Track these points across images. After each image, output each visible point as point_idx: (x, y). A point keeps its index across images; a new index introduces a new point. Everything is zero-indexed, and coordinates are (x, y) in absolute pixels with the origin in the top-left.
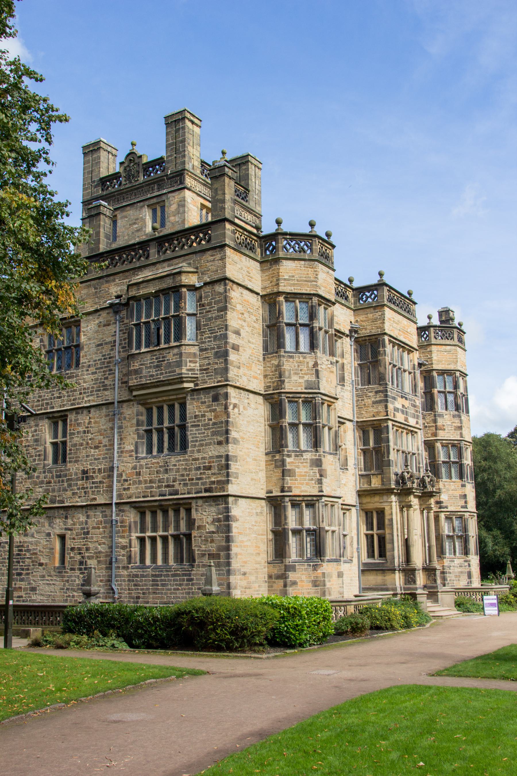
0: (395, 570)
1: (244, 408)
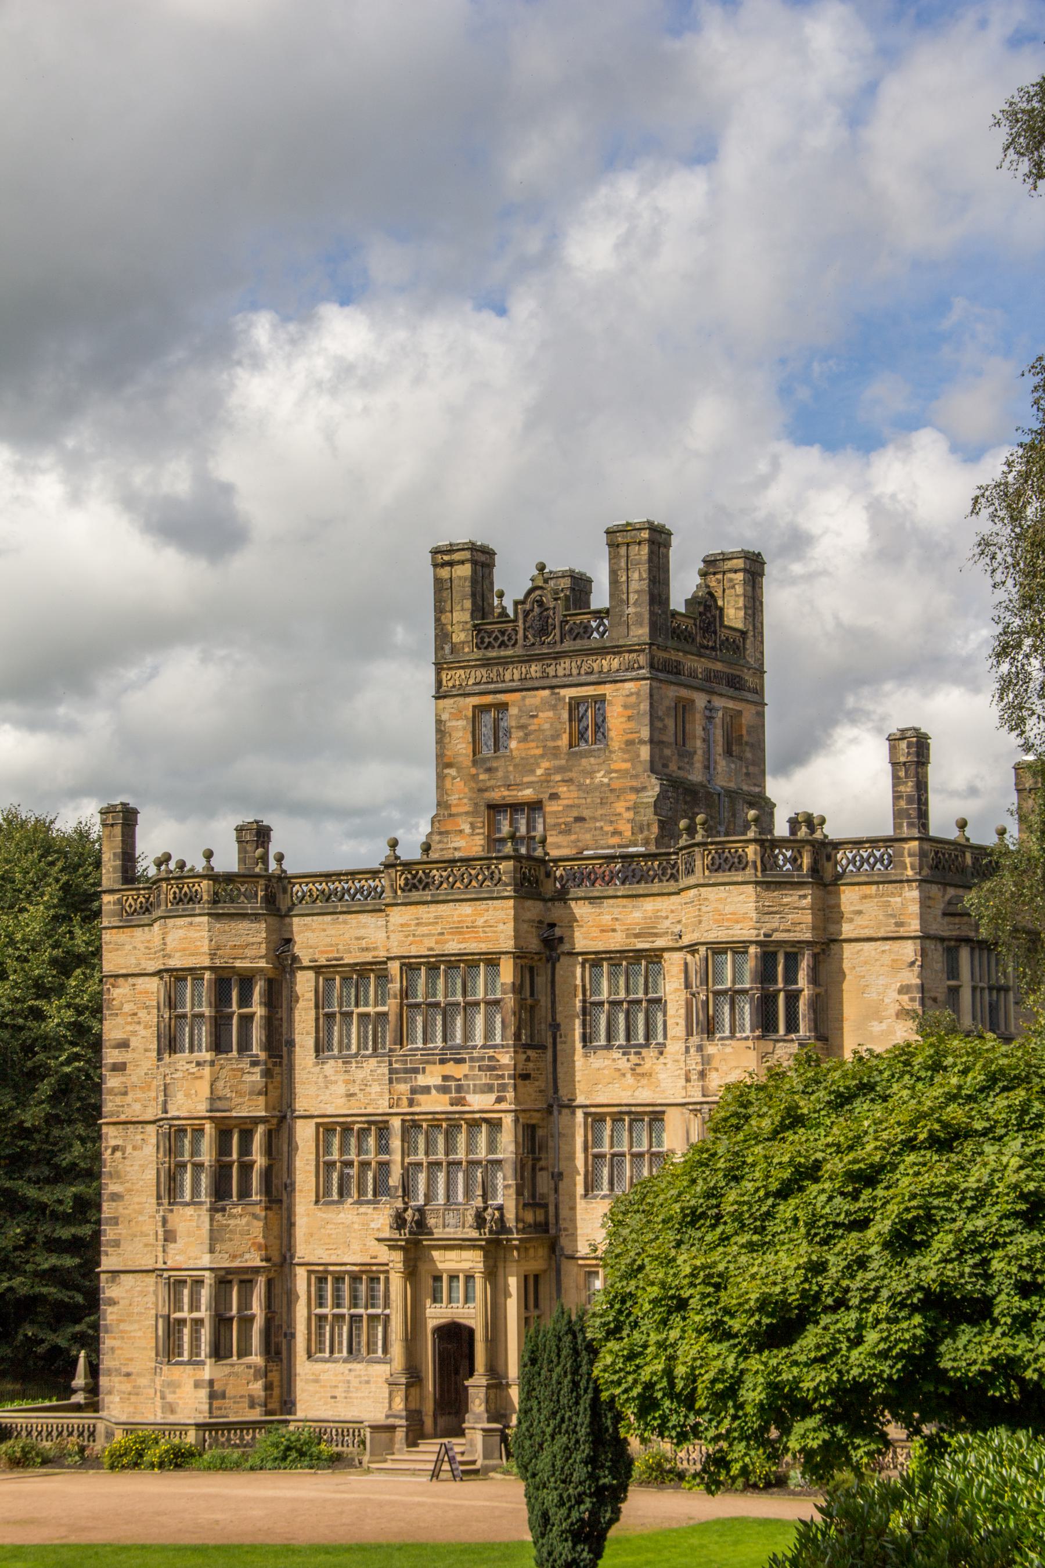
1: (135, 1148)
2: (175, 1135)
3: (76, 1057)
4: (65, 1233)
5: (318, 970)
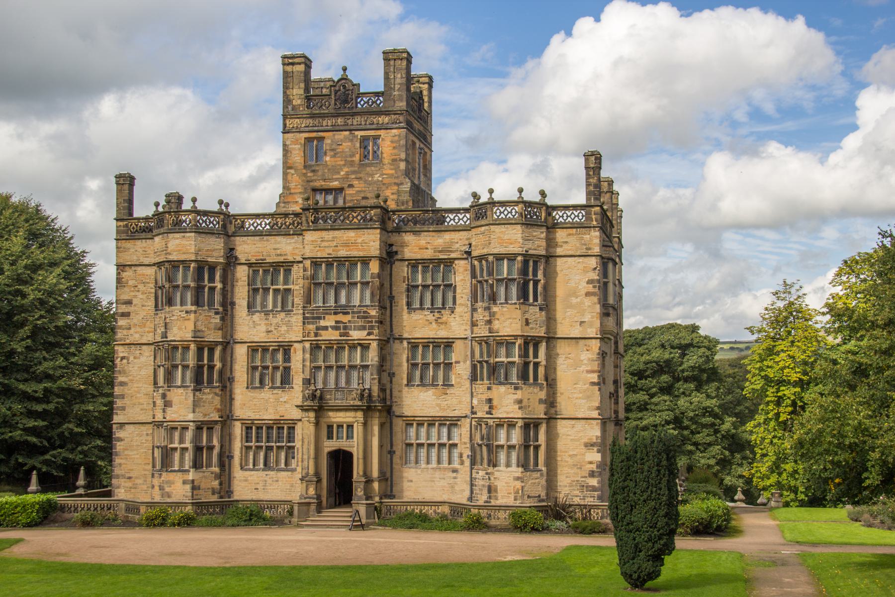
1: (135, 358)
2: (168, 351)
3: (41, 317)
4: (39, 408)
5: (250, 265)
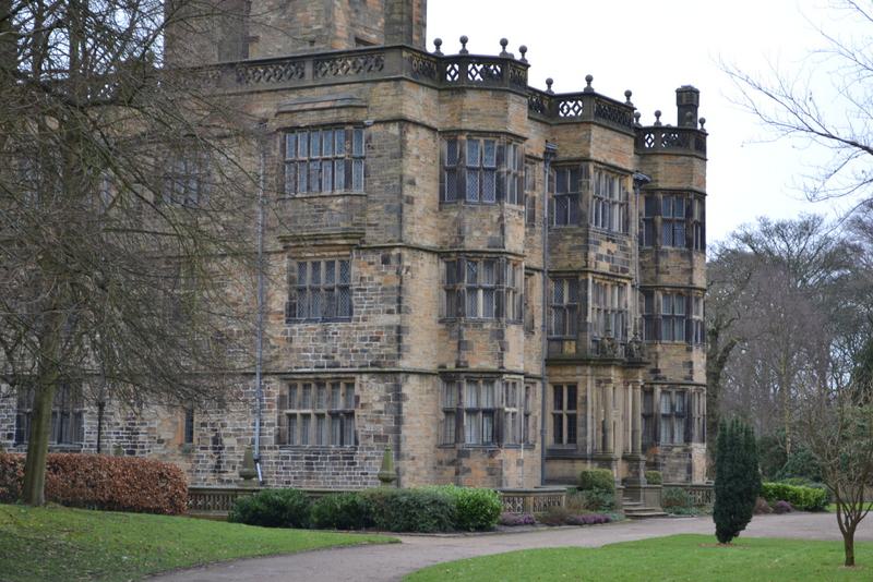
0: (586, 459)
